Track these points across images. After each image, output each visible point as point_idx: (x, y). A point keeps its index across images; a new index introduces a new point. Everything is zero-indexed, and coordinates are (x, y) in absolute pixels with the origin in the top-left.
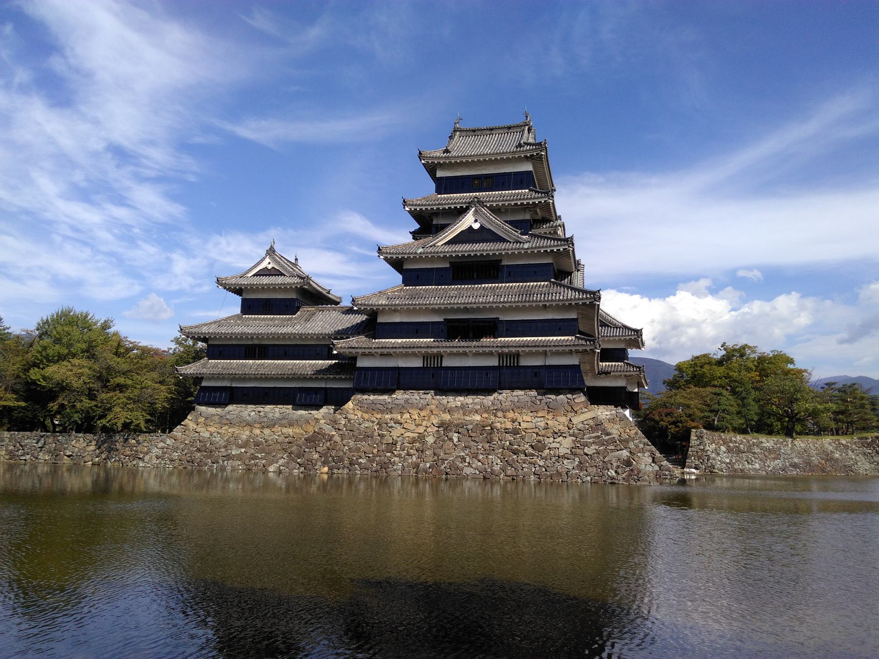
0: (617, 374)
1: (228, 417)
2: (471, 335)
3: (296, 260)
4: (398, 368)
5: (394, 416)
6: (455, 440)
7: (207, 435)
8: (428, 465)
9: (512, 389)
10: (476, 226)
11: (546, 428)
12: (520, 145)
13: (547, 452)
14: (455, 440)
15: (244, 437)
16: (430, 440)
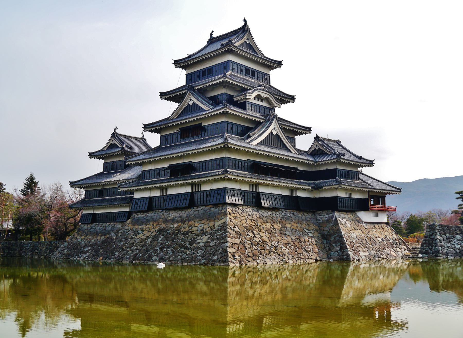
0: (326, 187)
1: (91, 230)
2: (180, 174)
3: (143, 135)
4: (151, 198)
5: (143, 226)
6: (160, 239)
7: (79, 240)
8: (141, 255)
9: (198, 206)
10: (191, 103)
11: (202, 230)
12: (222, 45)
13: (194, 245)
14: (160, 239)
15: (93, 241)
16: (149, 240)
